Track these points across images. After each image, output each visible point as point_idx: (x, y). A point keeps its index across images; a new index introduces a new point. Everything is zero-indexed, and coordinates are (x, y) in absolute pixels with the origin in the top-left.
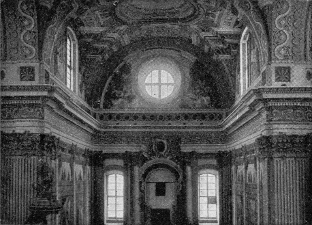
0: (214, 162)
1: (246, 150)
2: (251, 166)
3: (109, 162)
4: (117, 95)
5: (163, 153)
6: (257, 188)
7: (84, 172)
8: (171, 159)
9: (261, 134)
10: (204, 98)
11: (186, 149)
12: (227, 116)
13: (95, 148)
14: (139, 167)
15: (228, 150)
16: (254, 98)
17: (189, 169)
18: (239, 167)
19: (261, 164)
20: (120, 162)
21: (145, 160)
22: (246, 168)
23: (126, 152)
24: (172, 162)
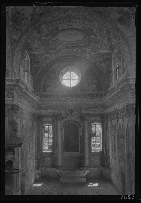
0: (99, 118)
1: (116, 112)
2: (121, 121)
3: (44, 119)
4: (49, 85)
5: (72, 114)
6: (124, 132)
7: (32, 125)
8: (77, 118)
9: (128, 103)
10: (93, 86)
11: (84, 112)
12: (105, 95)
13: (38, 112)
14: (60, 122)
15: (106, 112)
16: (125, 83)
17: (86, 122)
18: (113, 121)
19: (127, 119)
20: (50, 119)
21: (63, 118)
22: (118, 121)
23: (54, 114)
24: (77, 119)
